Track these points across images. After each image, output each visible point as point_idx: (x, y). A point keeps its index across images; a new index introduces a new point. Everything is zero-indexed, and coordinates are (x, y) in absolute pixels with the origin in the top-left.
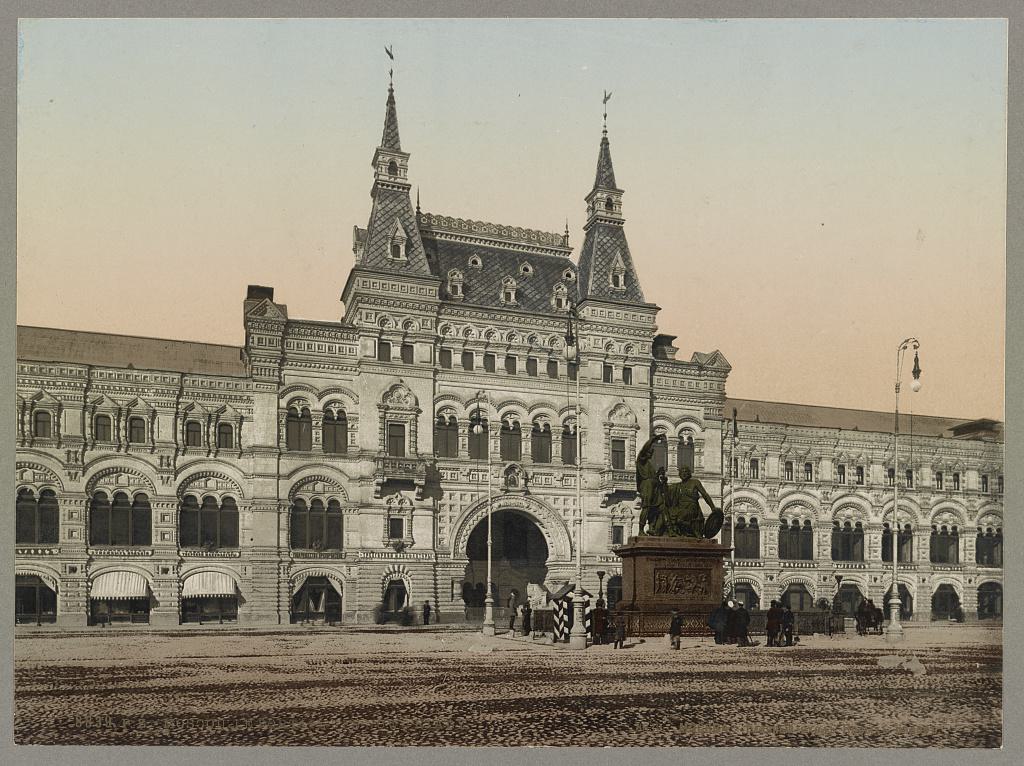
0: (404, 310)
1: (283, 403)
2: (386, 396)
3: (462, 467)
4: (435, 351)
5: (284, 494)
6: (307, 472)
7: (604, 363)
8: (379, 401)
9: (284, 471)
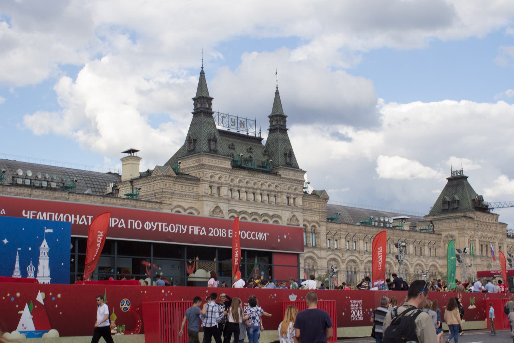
0: (218, 172)
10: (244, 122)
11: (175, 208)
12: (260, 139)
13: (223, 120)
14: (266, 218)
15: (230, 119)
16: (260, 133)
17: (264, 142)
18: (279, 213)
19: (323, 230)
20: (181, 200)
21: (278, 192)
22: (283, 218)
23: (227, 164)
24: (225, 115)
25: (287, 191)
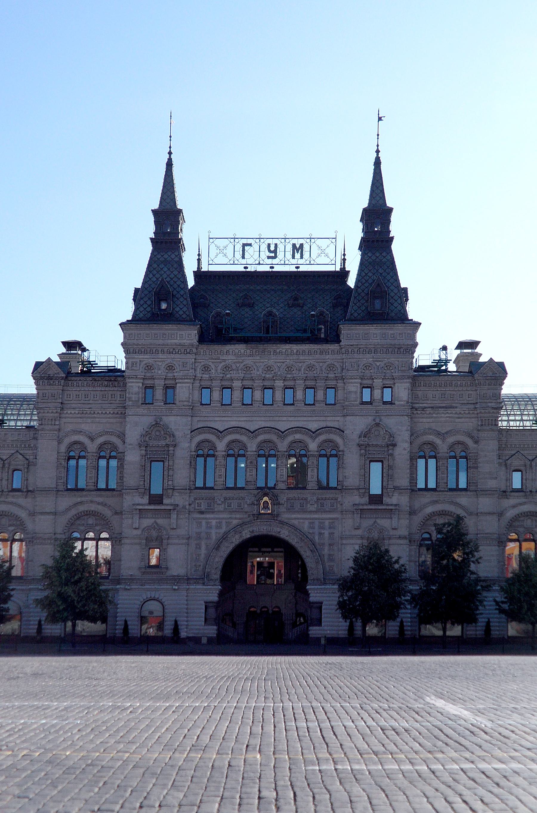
1: (63, 448)
3: (215, 494)
5: (59, 530)
6: (82, 508)
7: (361, 384)
10: (302, 245)
11: (66, 436)
13: (244, 250)
14: (298, 436)
15: (264, 247)
16: (344, 260)
24: (249, 241)
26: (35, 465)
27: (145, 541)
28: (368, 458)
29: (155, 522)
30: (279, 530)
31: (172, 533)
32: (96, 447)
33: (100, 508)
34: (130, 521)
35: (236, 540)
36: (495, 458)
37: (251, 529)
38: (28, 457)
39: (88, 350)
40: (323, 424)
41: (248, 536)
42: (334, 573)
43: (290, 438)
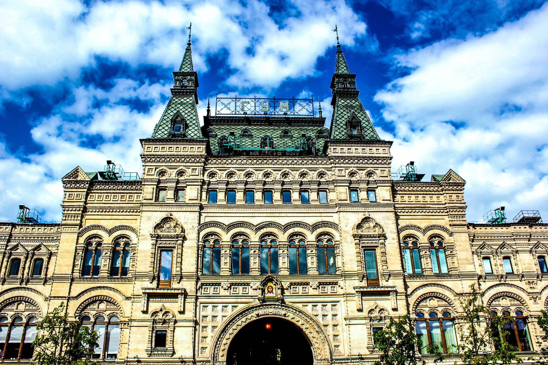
0: (178, 164)
1: (82, 240)
2: (158, 226)
4: (201, 192)
7: (349, 188)
8: (152, 231)
9: (74, 294)
12: (322, 121)
14: (297, 229)
17: (327, 125)
18: (335, 218)
19: (461, 241)
20: (104, 217)
21: (328, 183)
22: (342, 226)
23: (200, 150)
25: (347, 178)
26: (55, 254)
27: (151, 323)
28: (363, 247)
29: (163, 305)
30: (283, 312)
31: (179, 317)
32: (112, 239)
33: (111, 294)
34: (139, 304)
35: (242, 322)
36: (468, 246)
37: (257, 312)
38: (50, 248)
39: (113, 164)
40: (319, 219)
41: (254, 319)
42: (340, 353)
43: (291, 231)
